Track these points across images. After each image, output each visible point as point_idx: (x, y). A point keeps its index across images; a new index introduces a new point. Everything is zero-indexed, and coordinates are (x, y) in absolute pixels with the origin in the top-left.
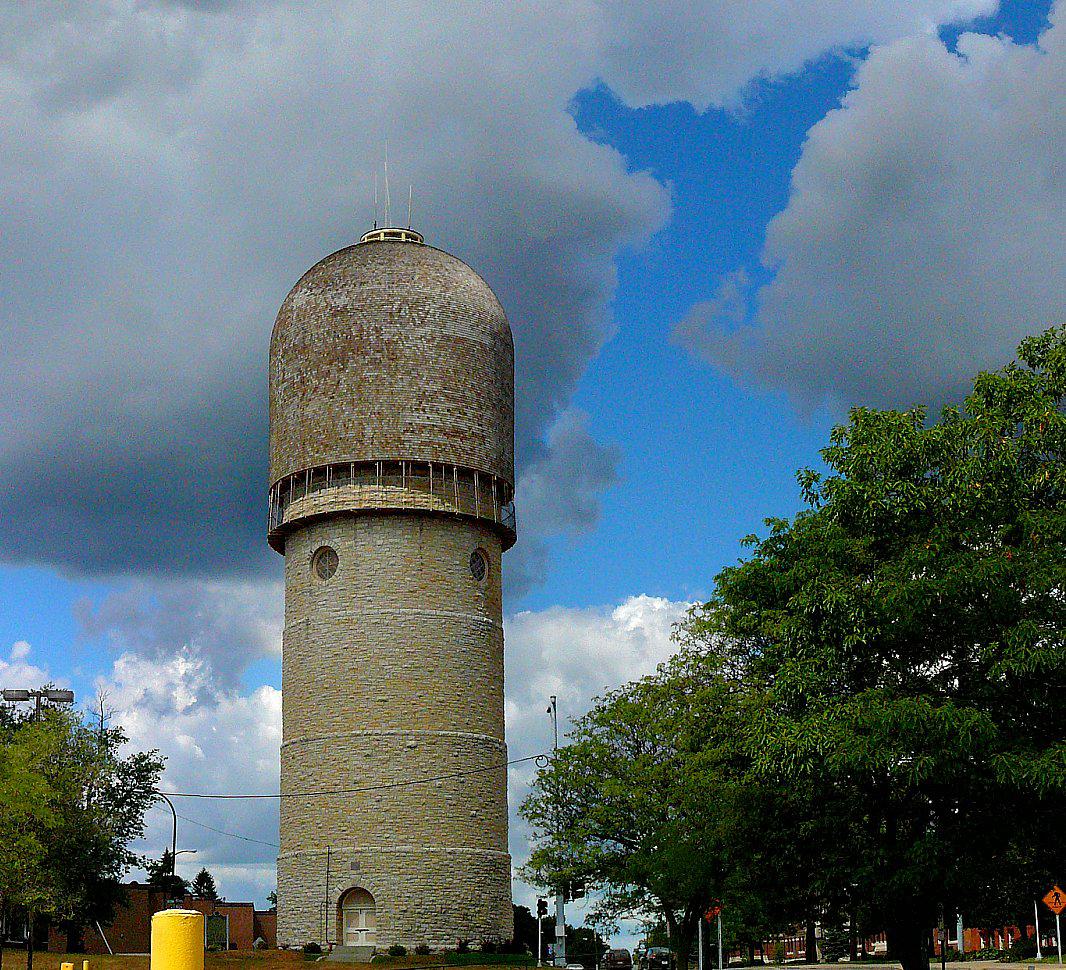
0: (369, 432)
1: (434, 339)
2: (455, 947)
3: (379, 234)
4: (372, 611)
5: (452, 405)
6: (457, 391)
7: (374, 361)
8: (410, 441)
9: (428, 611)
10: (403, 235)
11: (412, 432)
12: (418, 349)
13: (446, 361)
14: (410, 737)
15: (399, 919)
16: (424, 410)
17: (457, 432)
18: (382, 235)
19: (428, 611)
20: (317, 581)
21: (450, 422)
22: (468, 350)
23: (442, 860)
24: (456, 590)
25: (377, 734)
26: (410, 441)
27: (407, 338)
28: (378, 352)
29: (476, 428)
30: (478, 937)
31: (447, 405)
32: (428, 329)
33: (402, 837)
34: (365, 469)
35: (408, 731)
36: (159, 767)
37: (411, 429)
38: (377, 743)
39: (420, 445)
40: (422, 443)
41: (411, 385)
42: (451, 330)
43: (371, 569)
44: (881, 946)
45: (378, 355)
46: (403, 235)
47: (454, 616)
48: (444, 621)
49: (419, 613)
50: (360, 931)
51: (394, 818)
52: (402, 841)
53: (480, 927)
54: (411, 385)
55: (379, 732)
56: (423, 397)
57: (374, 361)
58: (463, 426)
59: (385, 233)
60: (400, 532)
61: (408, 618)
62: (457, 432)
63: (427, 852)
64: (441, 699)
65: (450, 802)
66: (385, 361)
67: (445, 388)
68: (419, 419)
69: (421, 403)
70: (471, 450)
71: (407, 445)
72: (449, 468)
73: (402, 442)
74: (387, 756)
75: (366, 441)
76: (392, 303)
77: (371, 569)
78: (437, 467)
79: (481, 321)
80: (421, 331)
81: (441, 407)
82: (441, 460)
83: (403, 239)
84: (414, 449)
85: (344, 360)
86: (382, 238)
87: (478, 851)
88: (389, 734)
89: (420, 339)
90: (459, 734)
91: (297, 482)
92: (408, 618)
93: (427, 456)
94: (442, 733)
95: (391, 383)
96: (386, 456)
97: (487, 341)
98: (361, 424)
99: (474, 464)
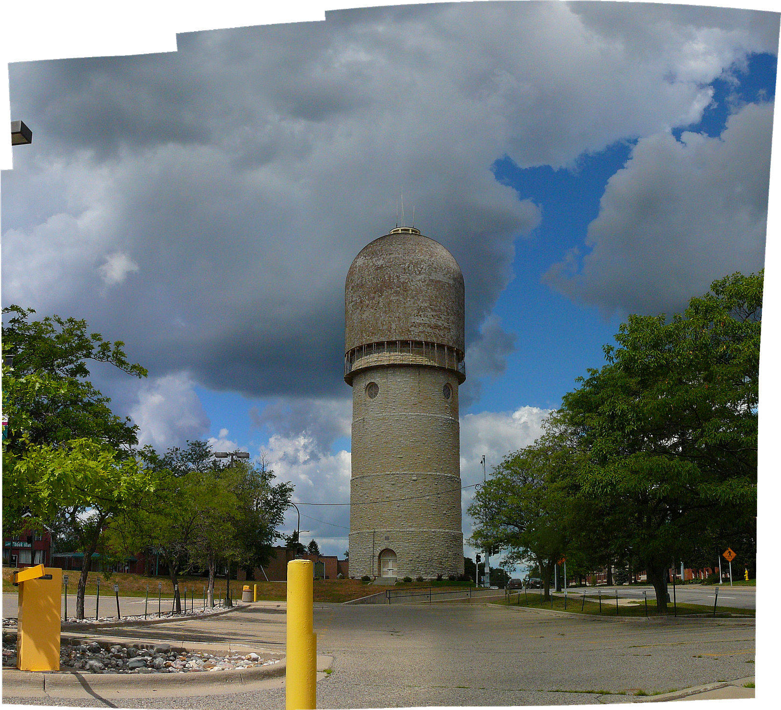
0: (394, 326)
1: (425, 281)
2: (436, 578)
3: (398, 230)
4: (395, 414)
5: (434, 313)
6: (437, 306)
7: (396, 292)
8: (413, 331)
9: (422, 414)
10: (410, 230)
11: (415, 326)
12: (418, 286)
14: (414, 475)
15: (408, 564)
16: (420, 316)
17: (437, 326)
18: (400, 230)
19: (422, 414)
20: (368, 399)
21: (433, 321)
22: (442, 286)
23: (429, 536)
25: (397, 474)
26: (413, 331)
27: (412, 281)
28: (398, 287)
29: (446, 325)
30: (447, 573)
31: (432, 313)
32: (422, 276)
33: (410, 524)
34: (392, 345)
35: (413, 473)
36: (291, 490)
37: (414, 325)
38: (397, 478)
39: (419, 333)
40: (420, 332)
41: (414, 304)
43: (395, 393)
44: (644, 577)
45: (398, 289)
46: (410, 230)
47: (435, 416)
48: (430, 418)
49: (418, 415)
50: (389, 570)
51: (406, 515)
52: (410, 526)
53: (448, 568)
54: (414, 304)
55: (398, 473)
56: (420, 309)
57: (396, 292)
58: (439, 323)
59: (402, 230)
60: (409, 375)
61: (413, 417)
62: (437, 326)
63: (422, 532)
64: (429, 457)
65: (433, 507)
66: (402, 292)
67: (431, 305)
68: (418, 320)
69: (419, 312)
70: (444, 335)
71: (412, 333)
72: (433, 344)
74: (402, 485)
75: (393, 331)
76: (405, 264)
77: (395, 393)
78: (427, 343)
80: (419, 277)
81: (429, 314)
82: (429, 340)
83: (410, 232)
87: (447, 531)
88: (403, 474)
89: (419, 281)
90: (438, 474)
91: (358, 351)
92: (413, 417)
93: (422, 338)
94: (429, 473)
95: (404, 303)
96: (402, 338)
97: (452, 282)
98: (390, 322)
99: (445, 342)
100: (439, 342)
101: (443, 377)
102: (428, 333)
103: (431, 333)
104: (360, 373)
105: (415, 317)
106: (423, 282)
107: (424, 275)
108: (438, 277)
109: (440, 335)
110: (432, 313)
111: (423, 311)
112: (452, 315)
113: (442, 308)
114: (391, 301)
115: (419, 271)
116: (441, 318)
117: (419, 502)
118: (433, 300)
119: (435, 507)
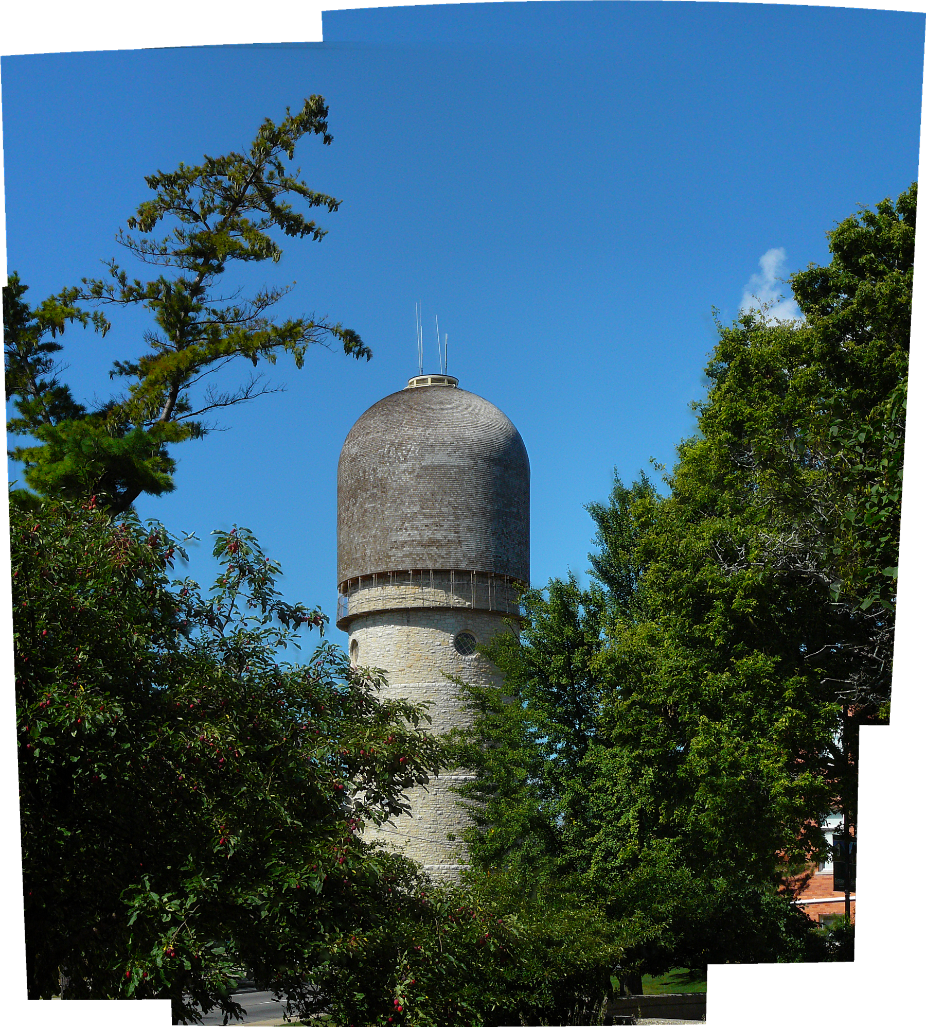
0: (368, 552)
3: (424, 381)
5: (430, 521)
6: (433, 509)
7: (373, 496)
9: (412, 685)
12: (402, 481)
13: (424, 486)
16: (406, 529)
17: (434, 542)
21: (428, 534)
22: (445, 474)
24: (438, 665)
26: (394, 556)
29: (452, 536)
31: (426, 522)
32: (410, 464)
34: (383, 578)
37: (397, 546)
41: (396, 510)
42: (428, 461)
54: (396, 510)
56: (404, 518)
57: (373, 496)
58: (439, 536)
59: (432, 379)
62: (434, 542)
65: (428, 830)
66: (379, 494)
67: (423, 509)
68: (402, 537)
69: (404, 523)
72: (428, 571)
73: (389, 557)
75: (367, 559)
76: (383, 447)
78: (416, 572)
79: (459, 448)
80: (404, 466)
81: (419, 524)
82: (419, 567)
84: (400, 561)
85: (355, 496)
86: (415, 385)
89: (404, 472)
91: (352, 585)
93: (409, 566)
96: (379, 570)
98: (364, 546)
99: (450, 564)
100: (438, 566)
101: (452, 621)
102: (418, 555)
103: (423, 554)
104: (355, 619)
105: (397, 531)
106: (410, 473)
107: (413, 461)
108: (440, 459)
109: (439, 556)
110: (426, 522)
111: (410, 521)
112: (466, 517)
113: (444, 509)
114: (366, 511)
115: (403, 455)
116: (442, 526)
117: (405, 824)
118: (428, 500)
119: (432, 830)
